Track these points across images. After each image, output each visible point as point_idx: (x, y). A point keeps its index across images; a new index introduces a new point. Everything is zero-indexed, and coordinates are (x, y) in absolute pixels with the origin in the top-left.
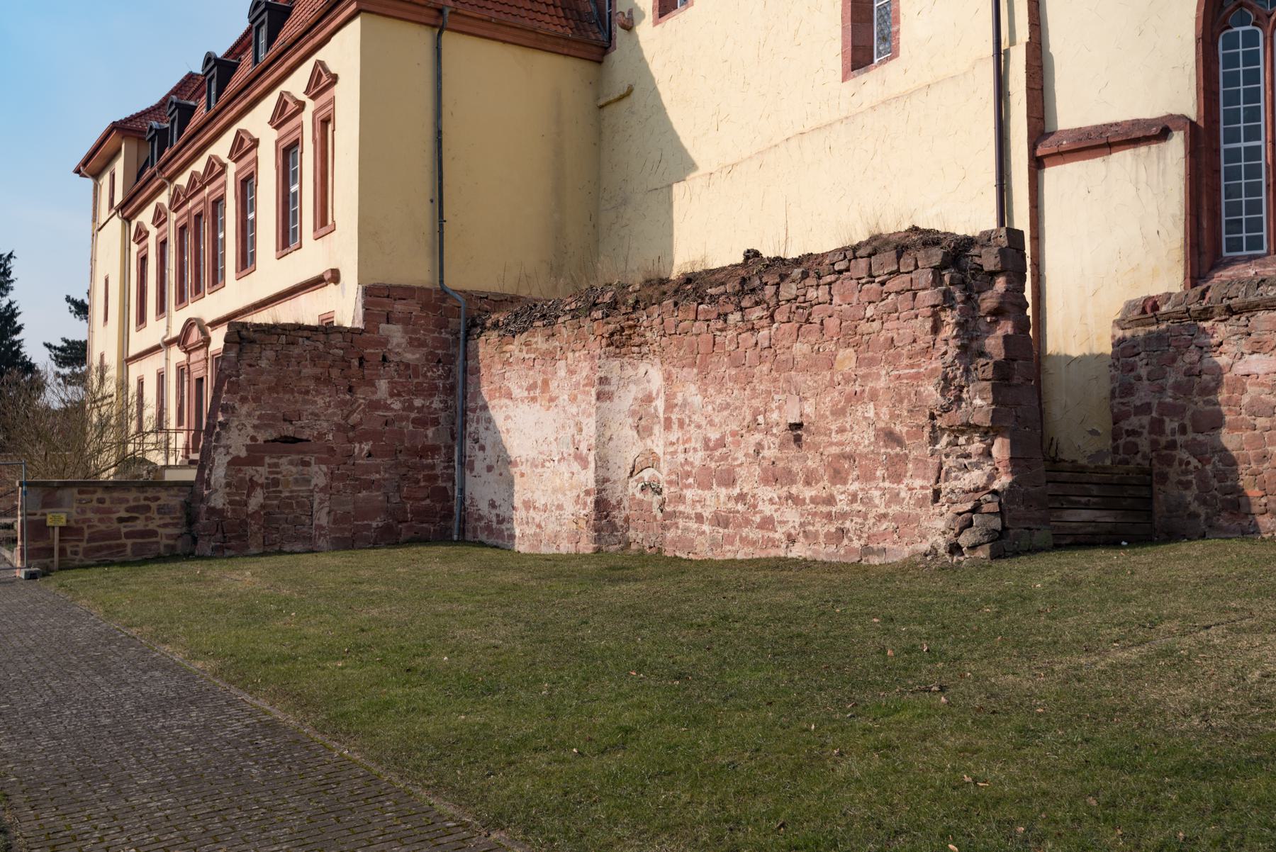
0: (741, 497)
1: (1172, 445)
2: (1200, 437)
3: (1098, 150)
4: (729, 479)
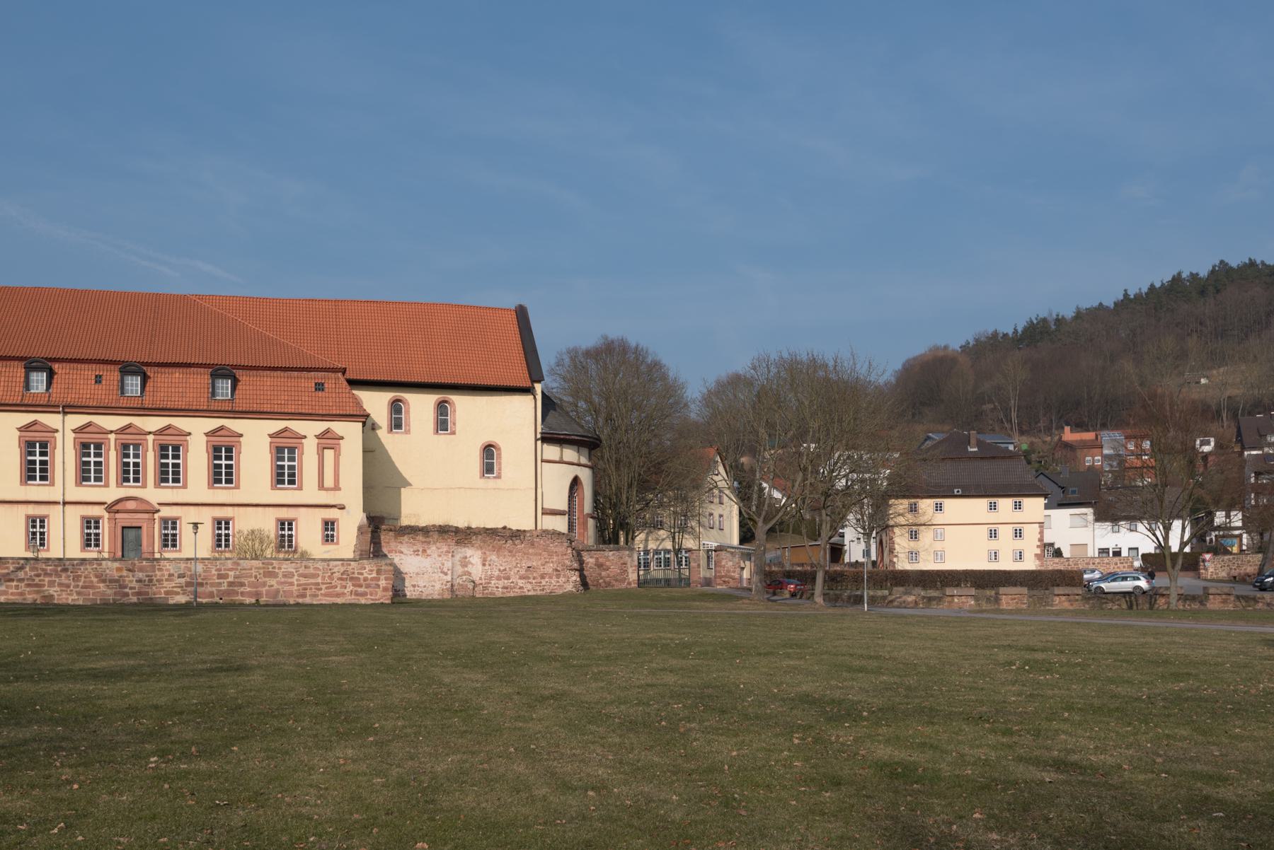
0: (512, 582)
4: (508, 578)
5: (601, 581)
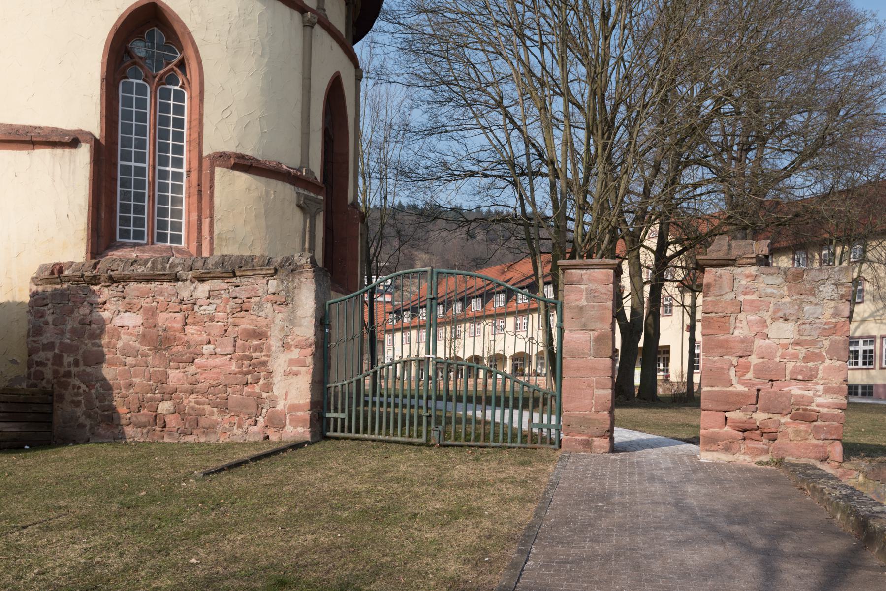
1: (68, 374)
2: (88, 369)
3: (22, 145)
5: (165, 407)
